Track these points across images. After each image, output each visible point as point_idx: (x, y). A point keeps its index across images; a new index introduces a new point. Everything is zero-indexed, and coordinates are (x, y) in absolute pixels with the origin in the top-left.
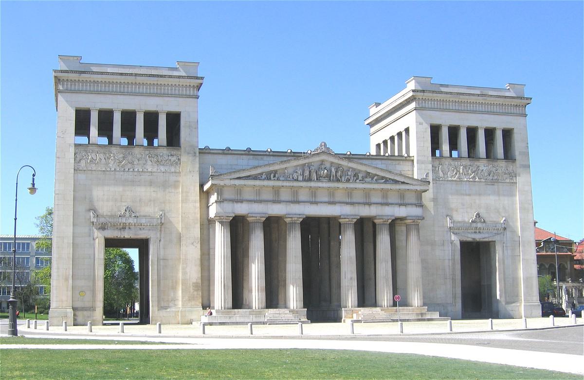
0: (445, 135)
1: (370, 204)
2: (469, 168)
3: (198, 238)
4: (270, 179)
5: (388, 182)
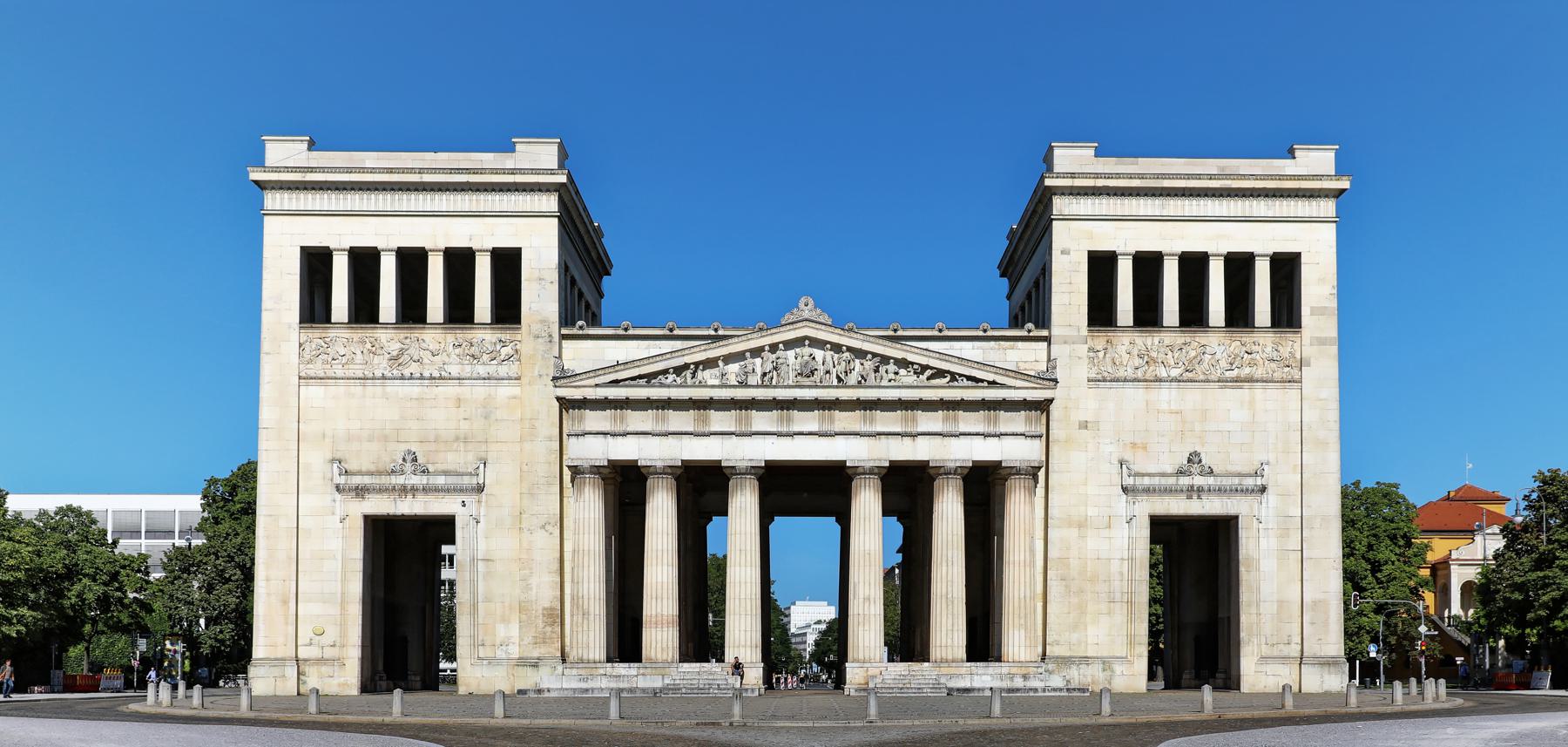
0: (1125, 273)
1: (914, 436)
3: (554, 514)
4: (685, 382)
5: (956, 383)
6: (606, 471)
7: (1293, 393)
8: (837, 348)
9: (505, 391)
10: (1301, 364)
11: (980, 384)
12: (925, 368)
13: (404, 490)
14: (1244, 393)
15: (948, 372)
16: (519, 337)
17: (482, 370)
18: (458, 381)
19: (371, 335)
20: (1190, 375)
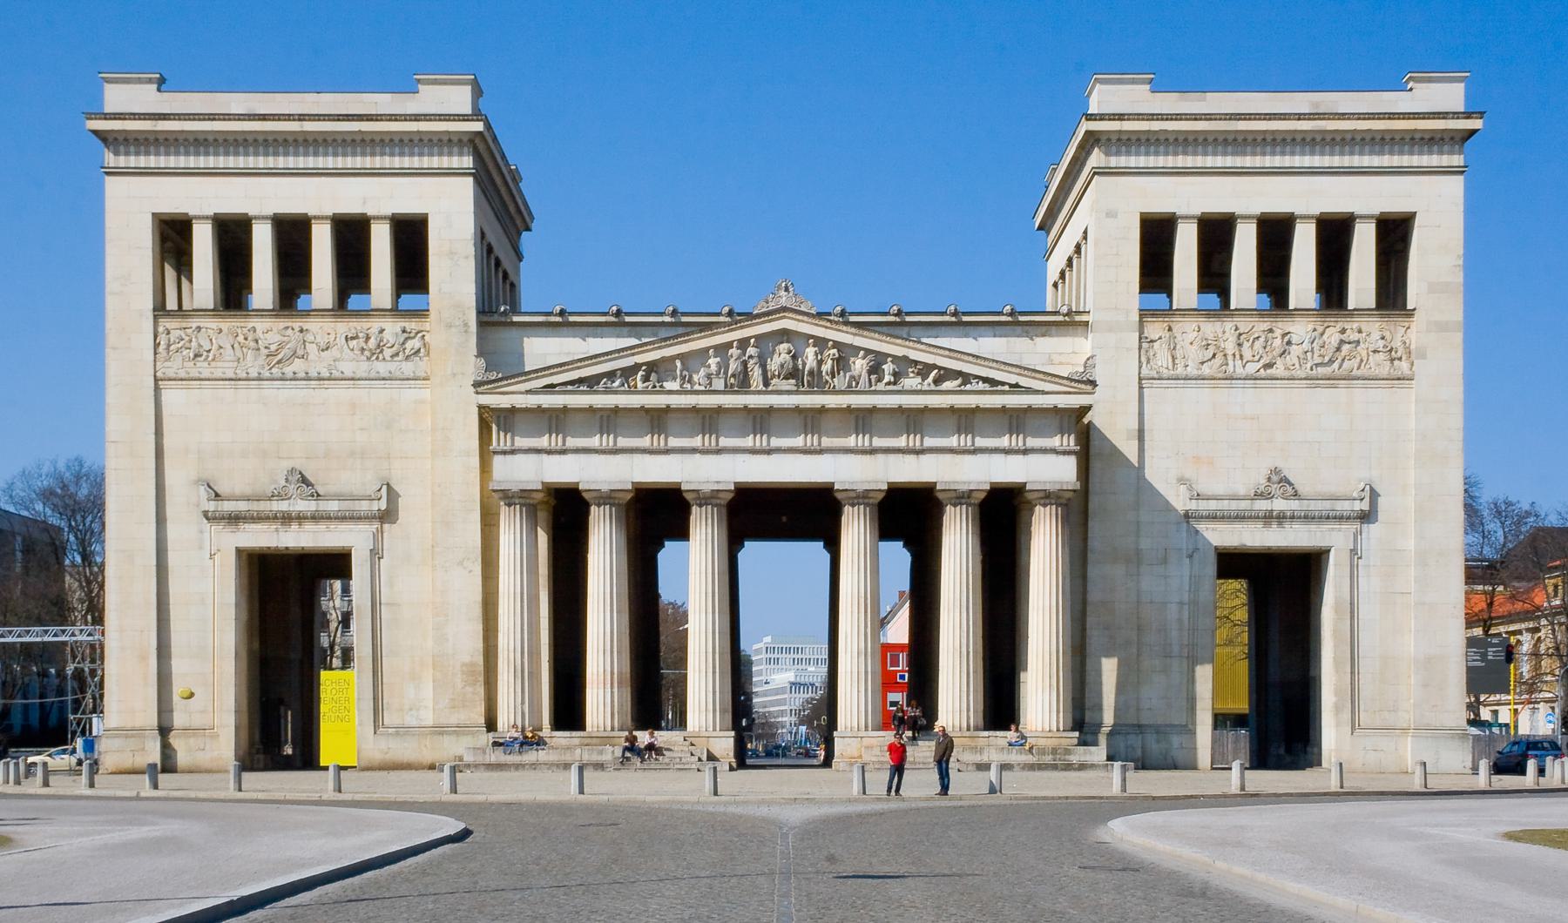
5: (968, 387)
6: (540, 496)
8: (821, 343)
9: (410, 394)
11: (1000, 388)
12: (934, 366)
13: (286, 519)
14: (1340, 394)
15: (959, 374)
16: (427, 326)
17: (382, 368)
18: (352, 382)
19: (242, 324)
20: (1269, 371)
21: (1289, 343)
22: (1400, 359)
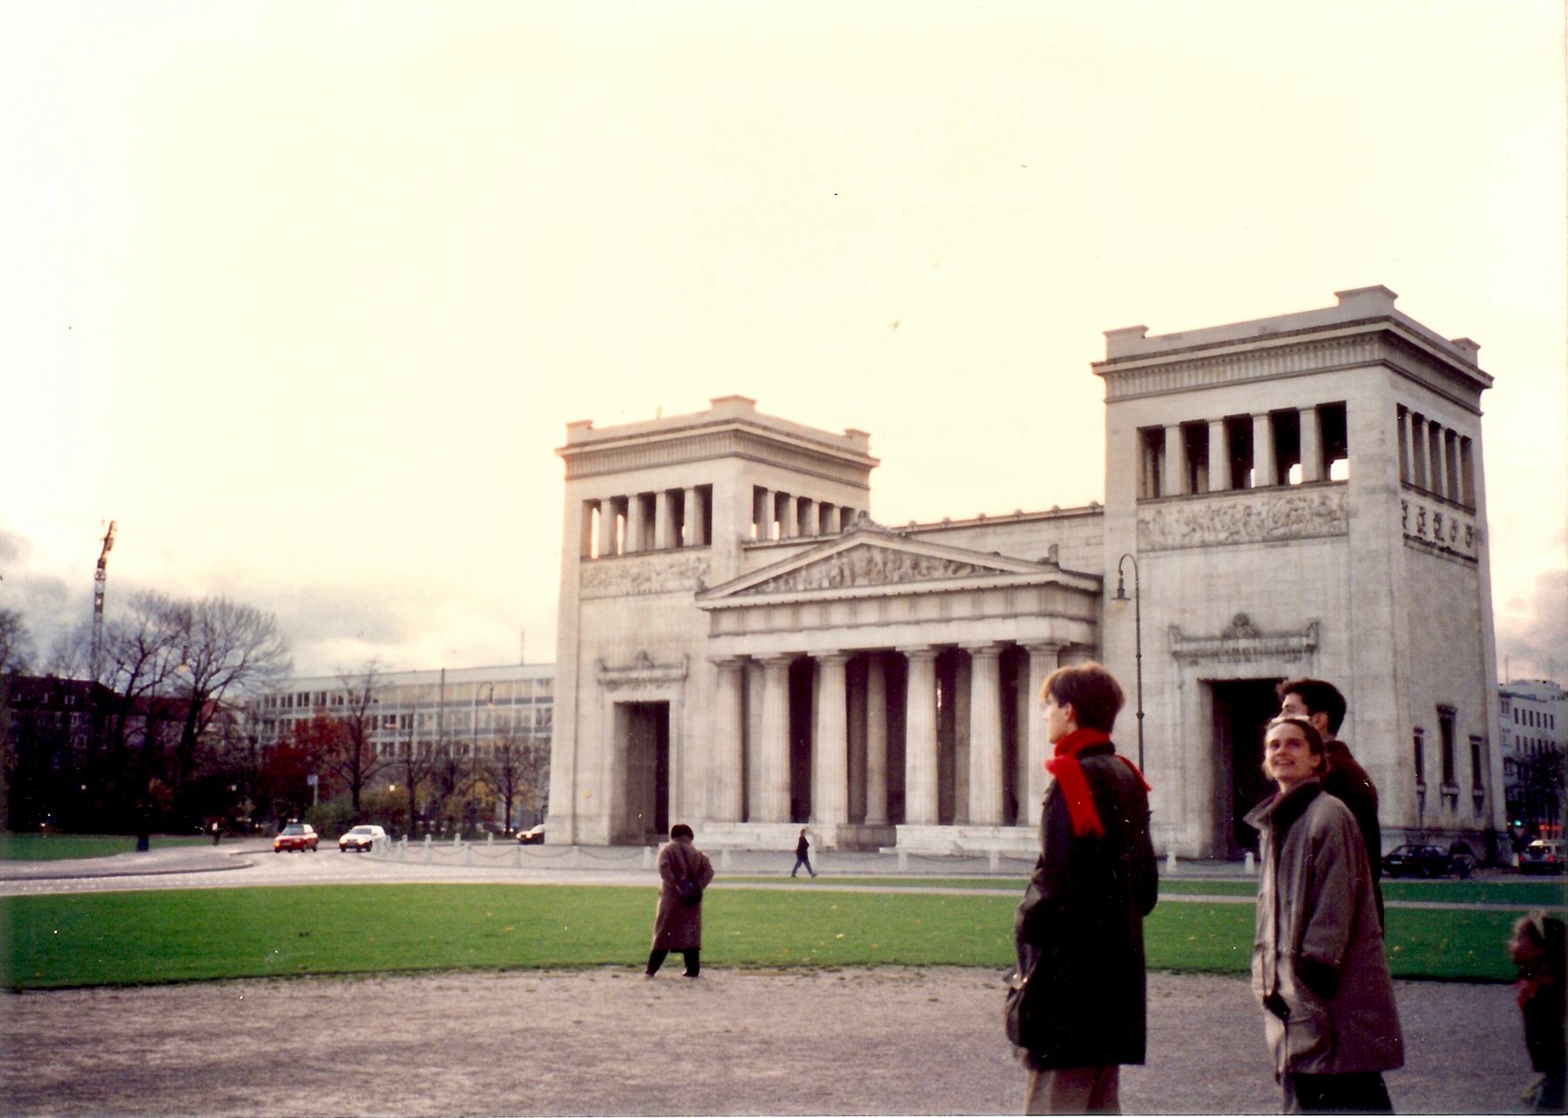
2: (1225, 513)
7: (1342, 548)
8: (884, 550)
10: (1348, 514)
20: (1236, 537)
21: (1249, 515)
22: (1338, 519)
